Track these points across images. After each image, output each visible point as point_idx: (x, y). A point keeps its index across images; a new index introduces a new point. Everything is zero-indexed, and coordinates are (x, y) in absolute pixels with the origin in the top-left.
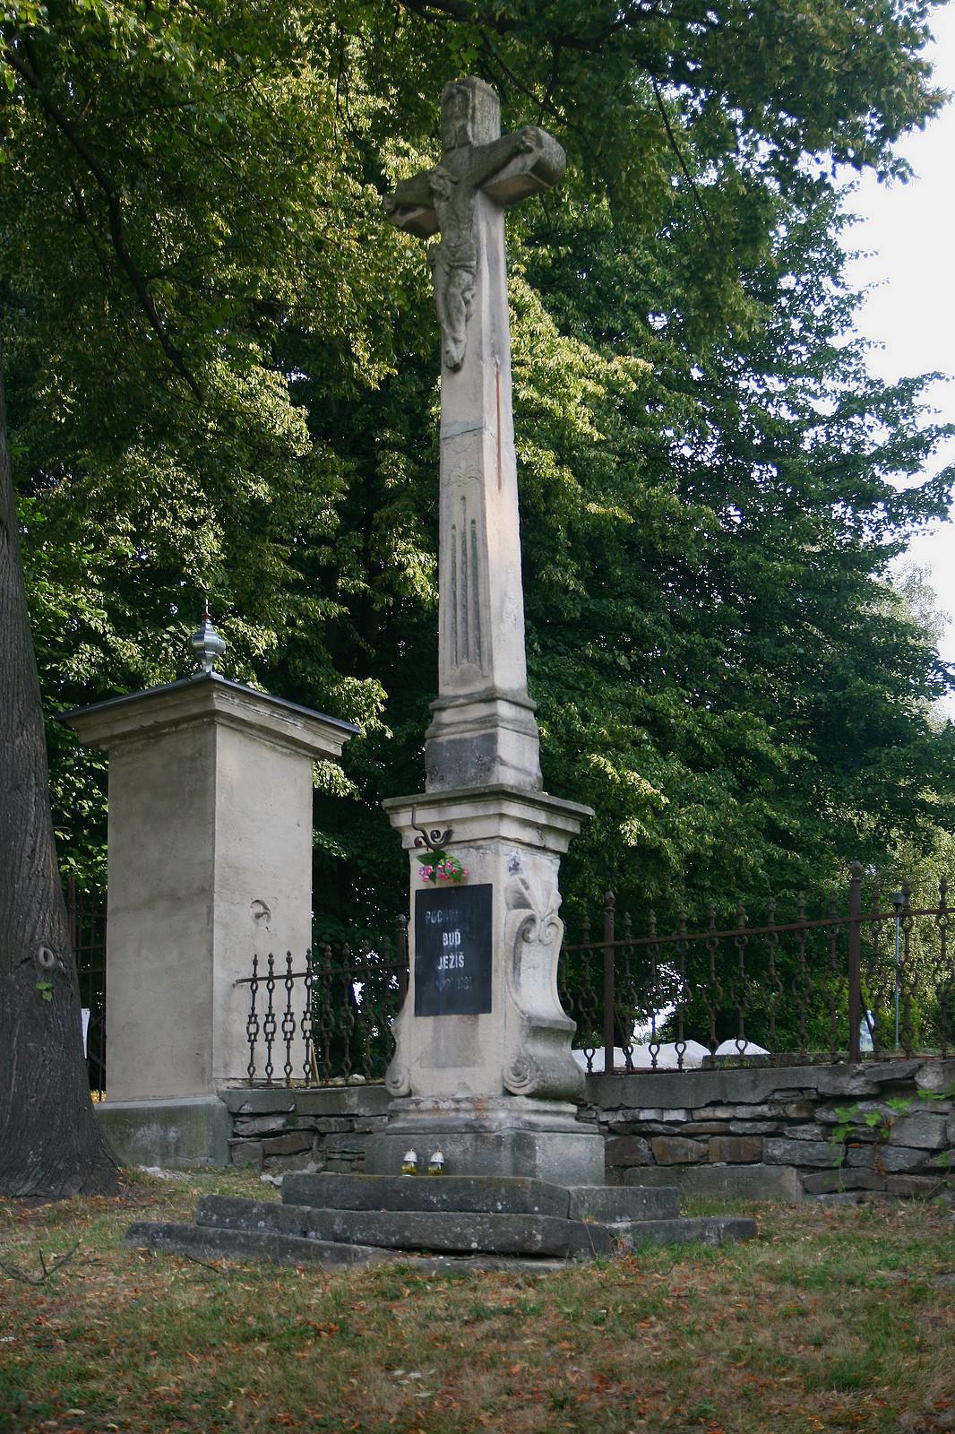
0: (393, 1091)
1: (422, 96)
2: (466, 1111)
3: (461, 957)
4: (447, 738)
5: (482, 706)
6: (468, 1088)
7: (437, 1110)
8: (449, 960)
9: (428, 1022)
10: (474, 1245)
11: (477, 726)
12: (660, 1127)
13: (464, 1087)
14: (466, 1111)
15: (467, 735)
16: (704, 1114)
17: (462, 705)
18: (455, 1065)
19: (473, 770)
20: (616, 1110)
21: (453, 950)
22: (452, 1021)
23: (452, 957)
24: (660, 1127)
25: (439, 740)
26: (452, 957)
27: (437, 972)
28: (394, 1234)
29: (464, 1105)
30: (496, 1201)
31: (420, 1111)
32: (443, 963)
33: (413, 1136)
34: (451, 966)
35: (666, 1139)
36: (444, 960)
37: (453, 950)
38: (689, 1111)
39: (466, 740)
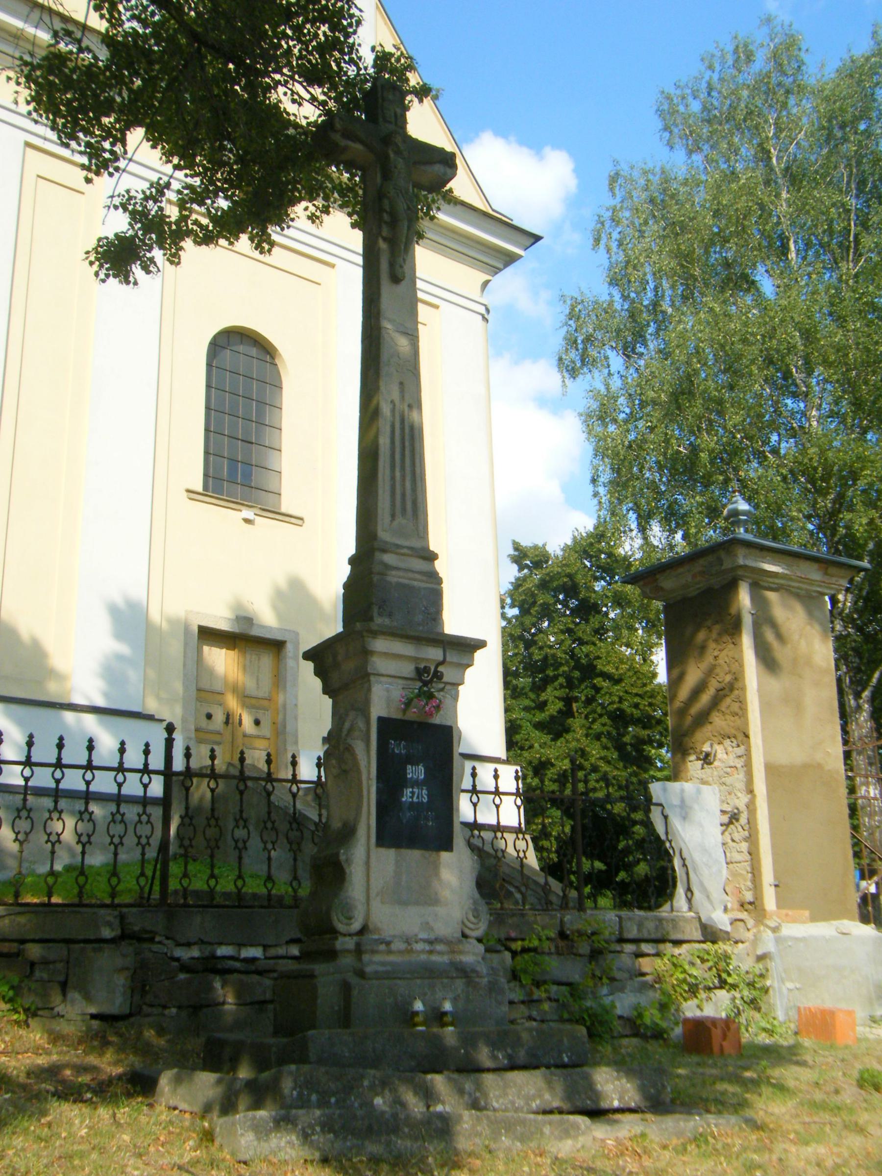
0: (341, 927)
1: (387, 76)
2: (440, 953)
3: (425, 792)
4: (395, 580)
5: (421, 561)
6: (432, 929)
7: (410, 951)
8: (413, 793)
9: (389, 855)
10: (616, 1104)
11: (424, 578)
12: (237, 965)
13: (427, 926)
14: (440, 953)
15: (415, 583)
16: (281, 951)
17: (403, 555)
18: (417, 903)
19: (421, 617)
20: (188, 945)
21: (416, 783)
22: (414, 855)
23: (416, 790)
24: (237, 965)
25: (389, 578)
26: (416, 790)
27: (401, 802)
28: (533, 1098)
29: (439, 947)
30: (560, 1053)
31: (390, 952)
32: (408, 795)
33: (399, 982)
34: (415, 799)
35: (243, 977)
36: (408, 791)
37: (416, 783)
38: (265, 947)
39: (414, 587)
